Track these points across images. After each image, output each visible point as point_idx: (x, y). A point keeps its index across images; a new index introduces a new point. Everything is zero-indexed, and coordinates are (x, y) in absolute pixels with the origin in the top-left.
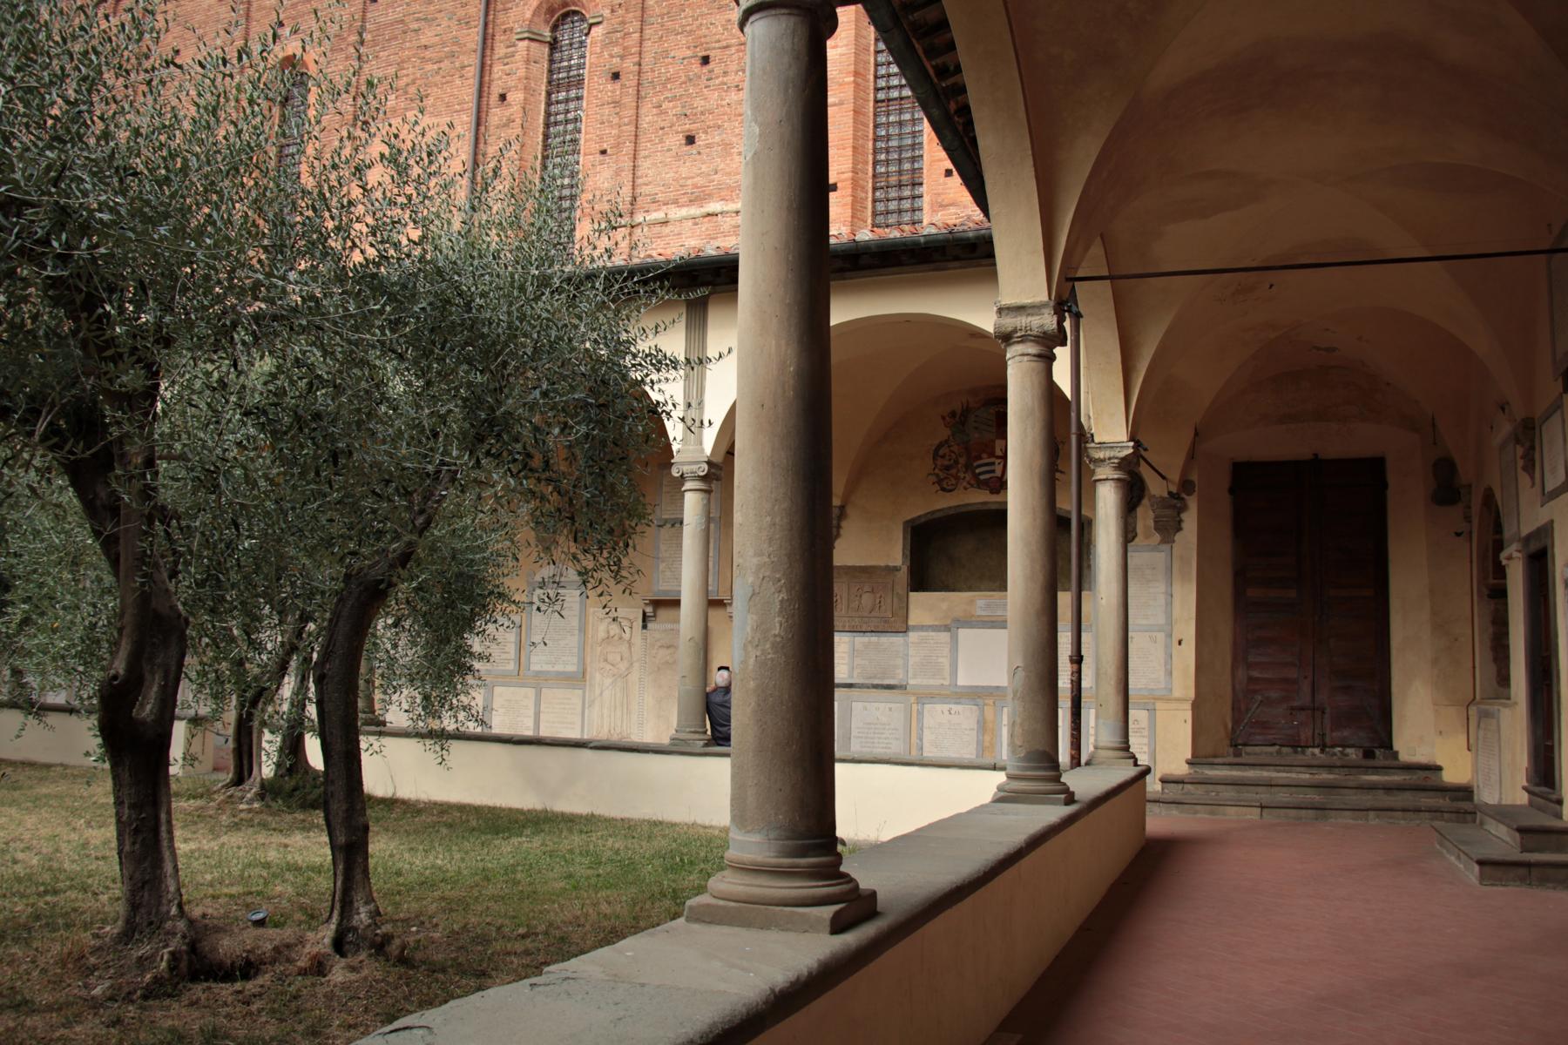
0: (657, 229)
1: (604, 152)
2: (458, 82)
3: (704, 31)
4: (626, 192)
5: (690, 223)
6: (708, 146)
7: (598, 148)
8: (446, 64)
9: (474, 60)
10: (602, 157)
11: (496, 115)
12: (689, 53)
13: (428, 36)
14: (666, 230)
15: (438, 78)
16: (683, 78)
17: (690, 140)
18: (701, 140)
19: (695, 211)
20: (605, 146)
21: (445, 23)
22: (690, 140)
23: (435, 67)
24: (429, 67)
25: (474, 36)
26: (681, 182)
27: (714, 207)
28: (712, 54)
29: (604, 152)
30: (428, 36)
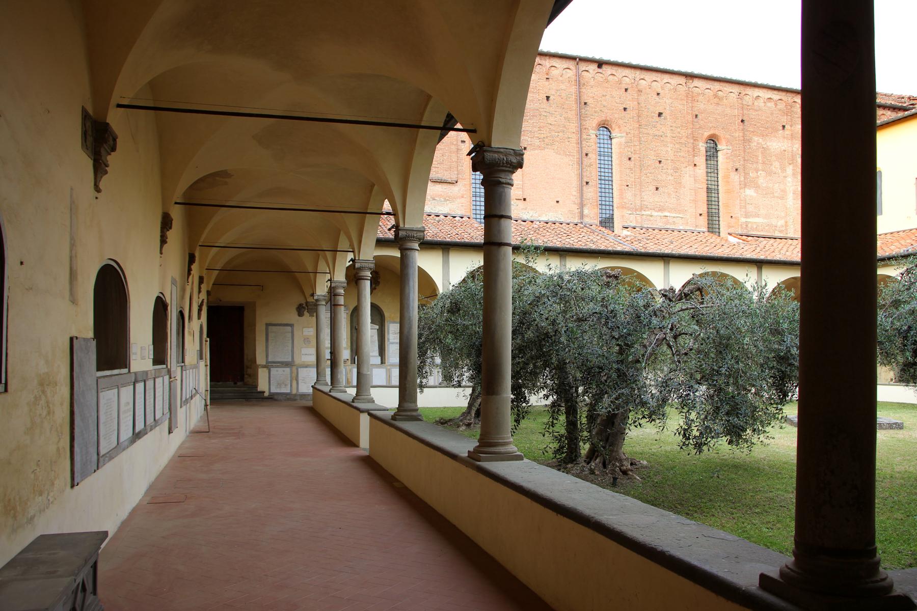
0: (648, 217)
1: (627, 186)
2: (567, 143)
3: (659, 152)
4: (638, 203)
5: (659, 217)
6: (664, 193)
7: (626, 184)
8: (561, 134)
9: (574, 138)
10: (627, 187)
11: (585, 160)
12: (655, 158)
13: (551, 120)
14: (651, 218)
15: (558, 139)
16: (654, 167)
17: (657, 189)
18: (661, 189)
19: (660, 214)
20: (628, 184)
21: (559, 117)
22: (657, 189)
23: (557, 134)
24: (554, 134)
25: (573, 126)
26: (656, 203)
27: (667, 214)
28: (663, 161)
29: (627, 186)
30: (551, 120)
